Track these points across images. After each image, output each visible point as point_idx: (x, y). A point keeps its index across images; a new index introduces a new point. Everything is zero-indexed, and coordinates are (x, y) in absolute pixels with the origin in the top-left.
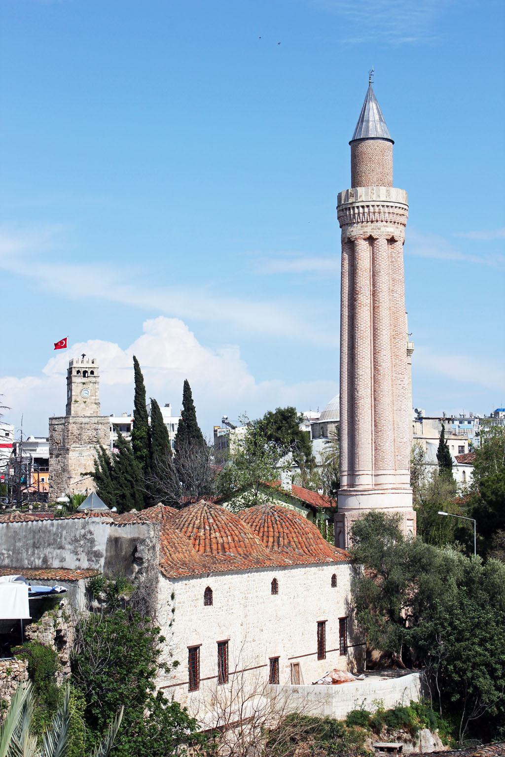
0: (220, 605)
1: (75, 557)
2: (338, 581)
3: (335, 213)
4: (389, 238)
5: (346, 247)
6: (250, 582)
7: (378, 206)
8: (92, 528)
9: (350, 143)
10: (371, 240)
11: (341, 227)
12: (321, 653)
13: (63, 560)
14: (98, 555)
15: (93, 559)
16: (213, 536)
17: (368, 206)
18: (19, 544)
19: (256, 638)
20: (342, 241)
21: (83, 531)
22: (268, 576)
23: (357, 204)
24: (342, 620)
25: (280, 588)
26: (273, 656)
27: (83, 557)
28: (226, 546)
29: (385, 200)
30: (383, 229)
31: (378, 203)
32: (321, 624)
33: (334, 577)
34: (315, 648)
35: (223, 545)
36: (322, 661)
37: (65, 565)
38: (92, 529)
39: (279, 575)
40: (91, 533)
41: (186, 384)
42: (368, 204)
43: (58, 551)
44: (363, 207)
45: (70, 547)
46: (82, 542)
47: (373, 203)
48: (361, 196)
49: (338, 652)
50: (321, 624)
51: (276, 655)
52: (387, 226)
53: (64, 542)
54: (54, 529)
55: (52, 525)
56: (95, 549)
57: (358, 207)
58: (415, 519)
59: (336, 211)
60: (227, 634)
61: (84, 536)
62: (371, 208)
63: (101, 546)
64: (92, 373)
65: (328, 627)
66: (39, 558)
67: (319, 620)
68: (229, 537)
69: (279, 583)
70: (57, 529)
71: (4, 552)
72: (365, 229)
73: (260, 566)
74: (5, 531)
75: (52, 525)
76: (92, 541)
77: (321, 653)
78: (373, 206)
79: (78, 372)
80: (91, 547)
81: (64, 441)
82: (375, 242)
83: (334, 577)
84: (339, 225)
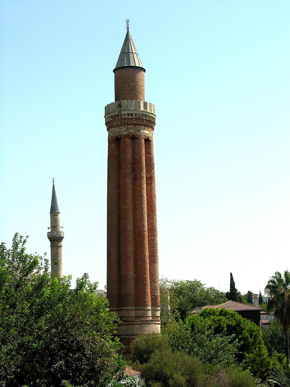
3: (103, 121)
4: (146, 138)
7: (139, 114)
11: (108, 130)
17: (132, 114)
30: (142, 131)
42: (132, 112)
44: (128, 114)
47: (136, 112)
48: (127, 107)
57: (124, 114)
62: (134, 115)
78: (136, 114)
82: (137, 141)
84: (106, 128)
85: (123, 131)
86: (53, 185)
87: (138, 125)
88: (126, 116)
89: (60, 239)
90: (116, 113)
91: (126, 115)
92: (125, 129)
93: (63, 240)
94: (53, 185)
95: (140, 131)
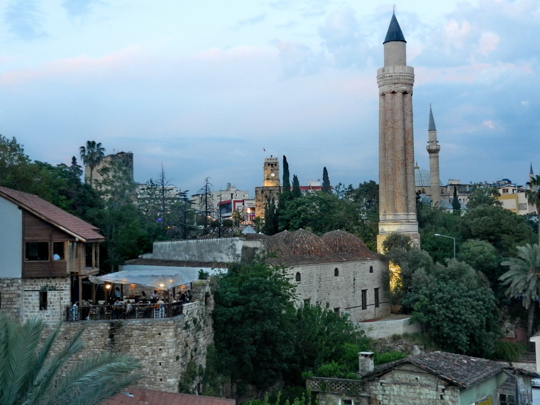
0: (305, 281)
1: (227, 257)
2: (374, 269)
3: (376, 80)
5: (382, 97)
6: (322, 270)
8: (235, 242)
9: (383, 43)
10: (394, 92)
11: (379, 87)
12: (364, 306)
13: (222, 258)
14: (238, 256)
15: (236, 258)
16: (304, 247)
18: (203, 250)
19: (326, 298)
20: (380, 95)
21: (231, 244)
22: (332, 267)
23: (388, 75)
24: (376, 290)
25: (340, 274)
26: (336, 307)
27: (231, 257)
28: (311, 252)
29: (401, 72)
31: (397, 74)
32: (364, 292)
33: (371, 268)
34: (360, 303)
35: (309, 251)
36: (364, 310)
37: (223, 261)
38: (235, 243)
39: (339, 266)
40: (234, 245)
41: (325, 169)
42: (392, 75)
43: (220, 254)
44: (389, 76)
45: (225, 252)
46: (230, 250)
47: (394, 74)
48: (388, 71)
49: (374, 306)
50: (364, 292)
51: (338, 307)
52: (402, 86)
53: (222, 249)
54: (218, 243)
55: (217, 241)
56: (237, 253)
58: (419, 238)
59: (376, 79)
60: (309, 296)
61: (232, 246)
63: (239, 252)
64: (276, 165)
65: (367, 293)
66: (211, 258)
67: (363, 289)
68: (313, 247)
69: (339, 270)
70: (219, 243)
71: (196, 254)
72: (391, 88)
73: (328, 261)
74: (196, 244)
75: (217, 241)
76: (235, 250)
77: (364, 306)
79: (269, 165)
80: (235, 252)
81: (262, 199)
83: (371, 268)
85: (386, 89)
86: (431, 108)
87: (397, 83)
88: (388, 78)
89: (436, 151)
90: (382, 76)
91: (388, 77)
92: (388, 87)
93: (440, 152)
94: (431, 108)
95: (398, 88)
